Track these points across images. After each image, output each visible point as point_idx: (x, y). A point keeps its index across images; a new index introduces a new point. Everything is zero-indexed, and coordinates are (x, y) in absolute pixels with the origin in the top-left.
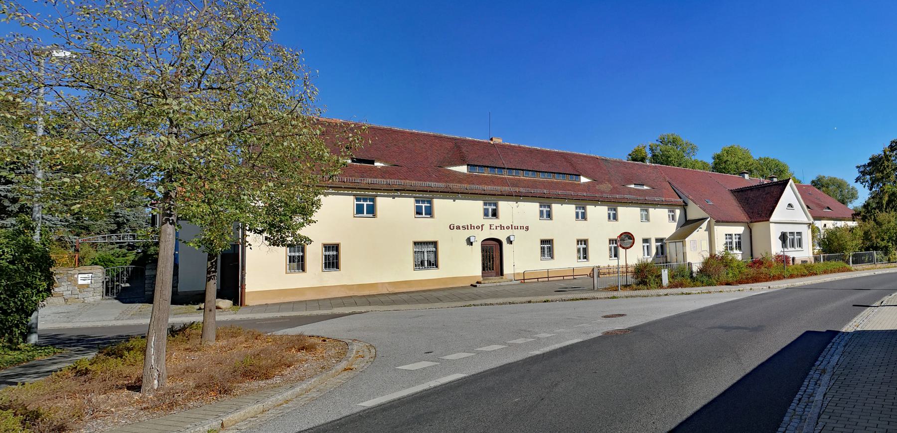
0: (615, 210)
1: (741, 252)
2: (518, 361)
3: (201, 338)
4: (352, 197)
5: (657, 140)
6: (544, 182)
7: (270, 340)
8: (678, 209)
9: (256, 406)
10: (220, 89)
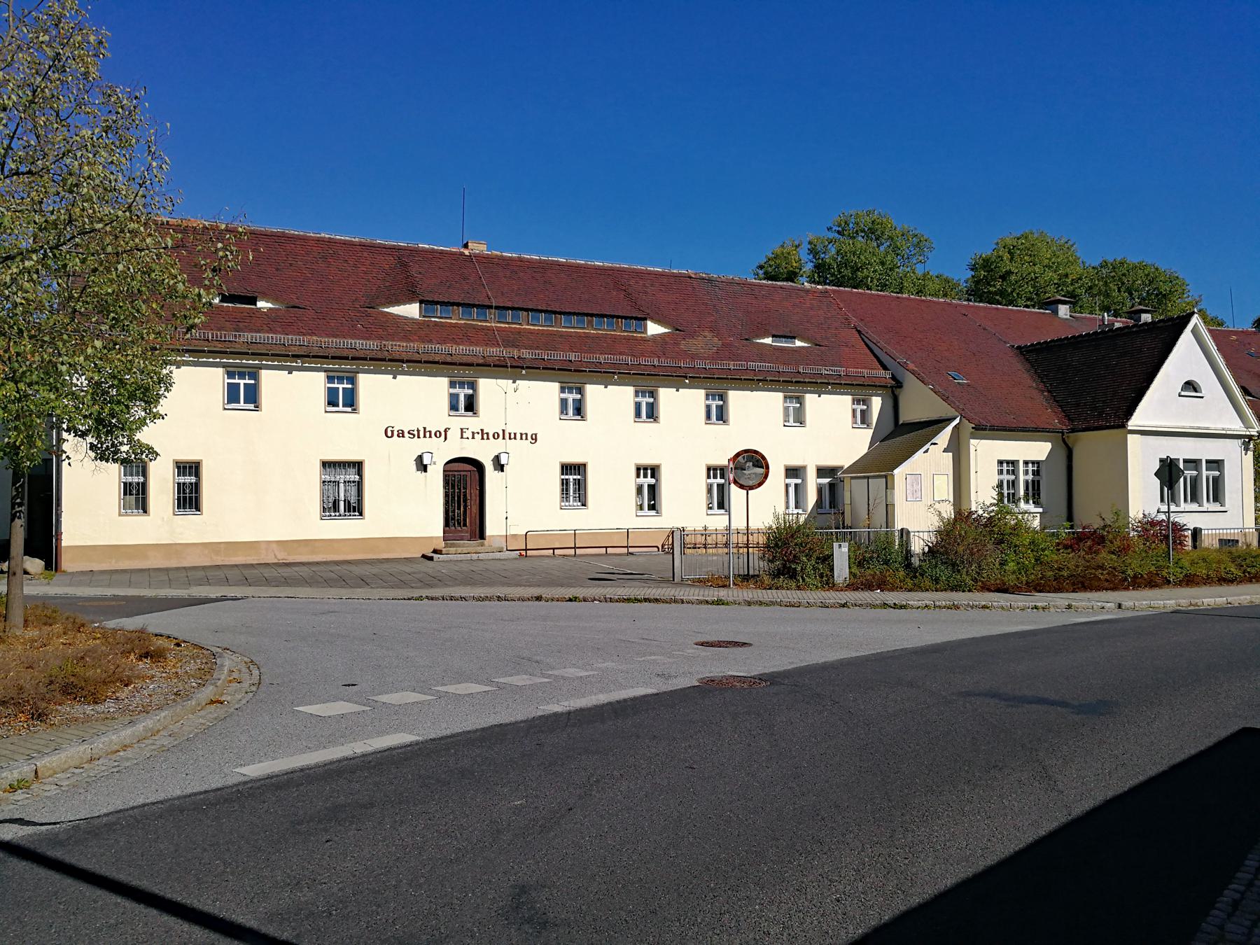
0: (722, 397)
1: (1040, 510)
2: (516, 722)
3: (5, 621)
4: (221, 370)
5: (829, 229)
6: (570, 335)
7: (99, 635)
8: (877, 395)
9: (82, 748)
10: (30, 172)
